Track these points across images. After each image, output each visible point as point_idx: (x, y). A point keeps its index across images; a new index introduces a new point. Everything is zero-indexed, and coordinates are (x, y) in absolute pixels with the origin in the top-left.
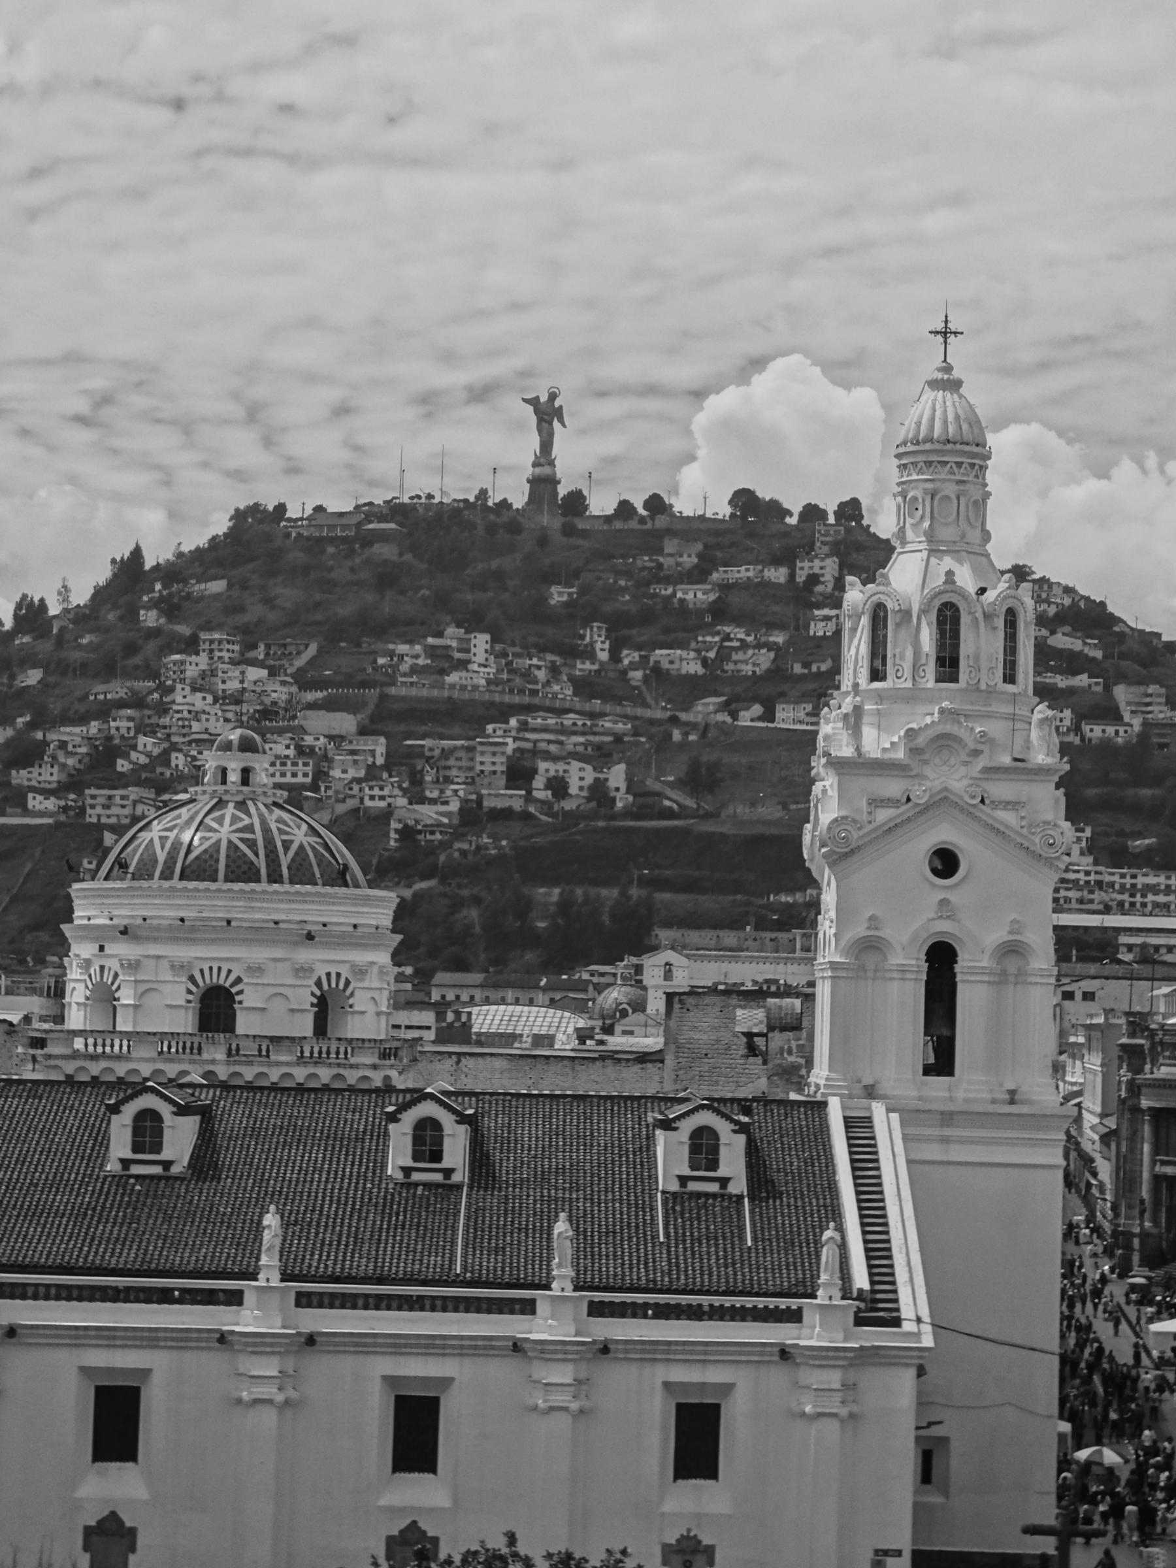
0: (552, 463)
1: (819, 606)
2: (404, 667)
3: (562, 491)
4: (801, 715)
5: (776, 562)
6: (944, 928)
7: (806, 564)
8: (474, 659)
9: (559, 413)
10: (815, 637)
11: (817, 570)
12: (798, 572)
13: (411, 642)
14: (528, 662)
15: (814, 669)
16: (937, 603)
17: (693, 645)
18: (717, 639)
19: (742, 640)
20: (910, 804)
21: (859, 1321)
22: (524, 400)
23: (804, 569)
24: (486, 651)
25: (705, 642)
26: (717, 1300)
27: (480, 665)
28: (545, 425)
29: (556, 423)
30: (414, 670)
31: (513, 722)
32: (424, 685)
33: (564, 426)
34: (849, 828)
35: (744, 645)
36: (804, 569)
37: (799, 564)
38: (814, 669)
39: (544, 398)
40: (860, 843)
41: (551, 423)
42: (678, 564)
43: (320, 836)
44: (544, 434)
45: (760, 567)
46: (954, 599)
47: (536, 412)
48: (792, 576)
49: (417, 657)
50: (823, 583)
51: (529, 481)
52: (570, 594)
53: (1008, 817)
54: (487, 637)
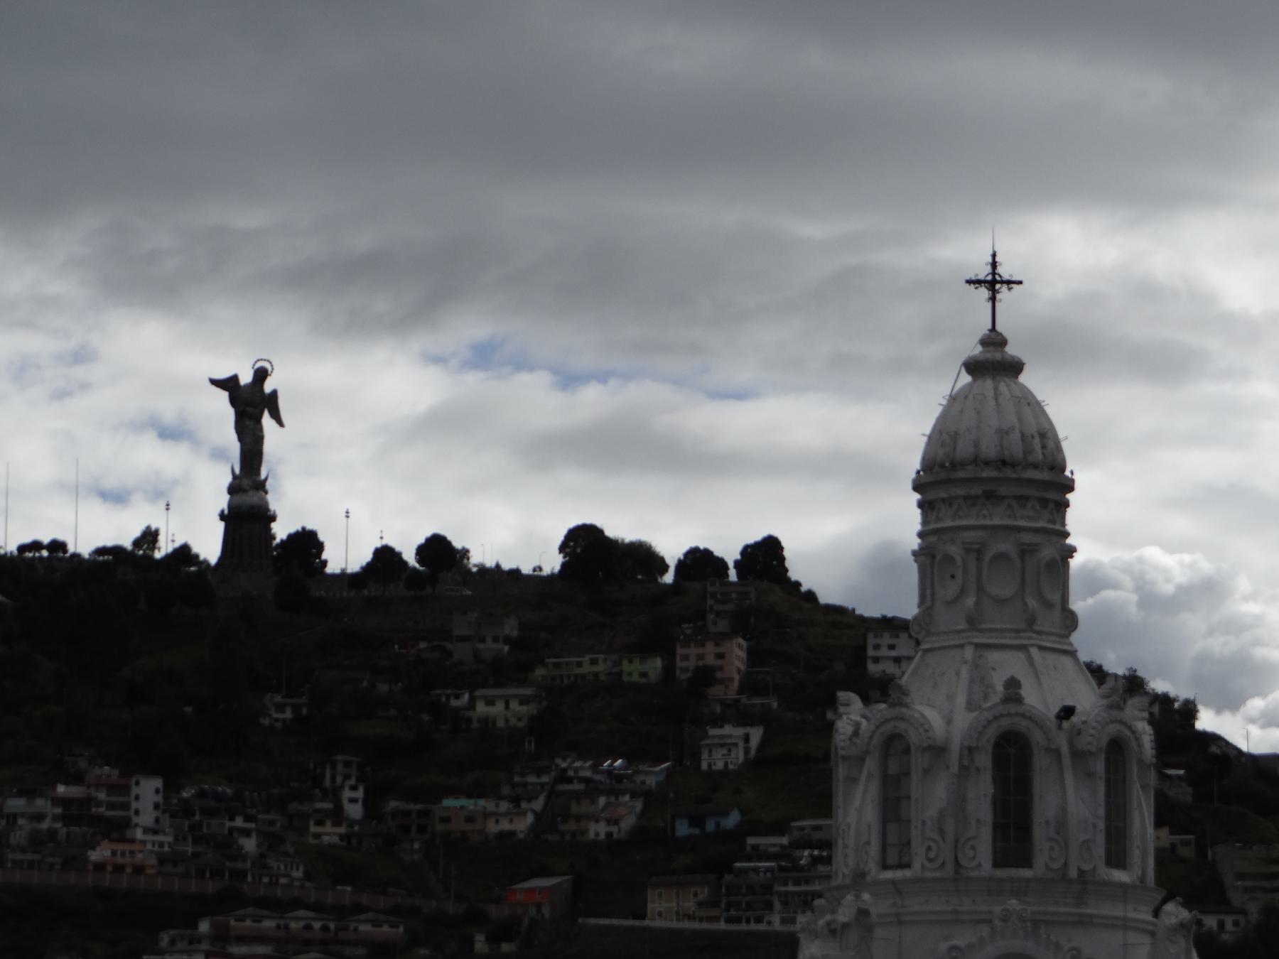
0: (261, 486)
1: (719, 722)
2: (19, 836)
4: (690, 905)
5: (644, 649)
7: (693, 651)
8: (135, 820)
9: (271, 403)
10: (711, 773)
11: (710, 660)
12: (679, 664)
13: (29, 793)
14: (228, 824)
15: (710, 826)
16: (992, 733)
17: (506, 790)
18: (545, 779)
19: (587, 781)
22: (215, 383)
23: (689, 658)
24: (156, 806)
25: (525, 785)
27: (147, 831)
28: (248, 423)
29: (267, 420)
30: (37, 841)
31: (204, 926)
32: (52, 866)
33: (281, 424)
35: (593, 788)
36: (689, 658)
37: (680, 651)
38: (710, 826)
39: (246, 378)
42: (476, 655)
45: (615, 657)
46: (1023, 724)
47: (233, 401)
48: (669, 670)
49: (40, 817)
50: (722, 681)
52: (296, 708)
54: (158, 783)
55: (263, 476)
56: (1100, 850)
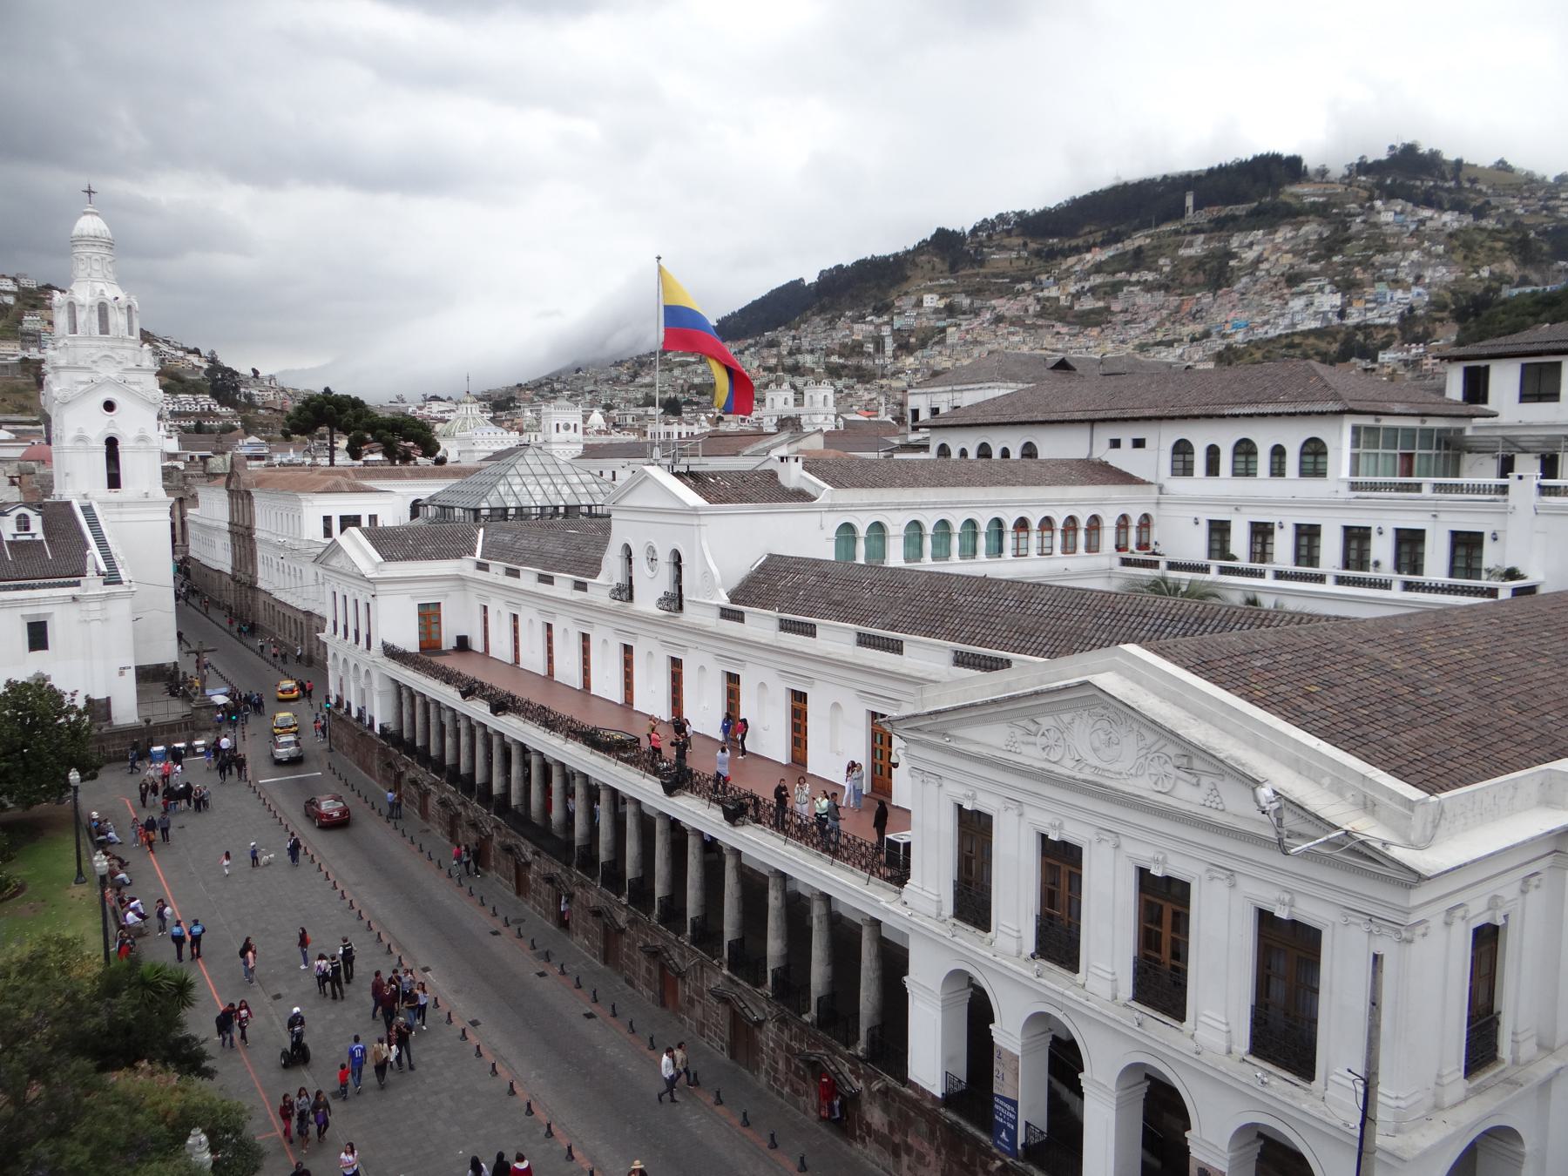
6: (112, 432)
16: (97, 303)
21: (105, 584)
26: (42, 581)
46: (105, 301)
53: (136, 388)
56: (127, 331)
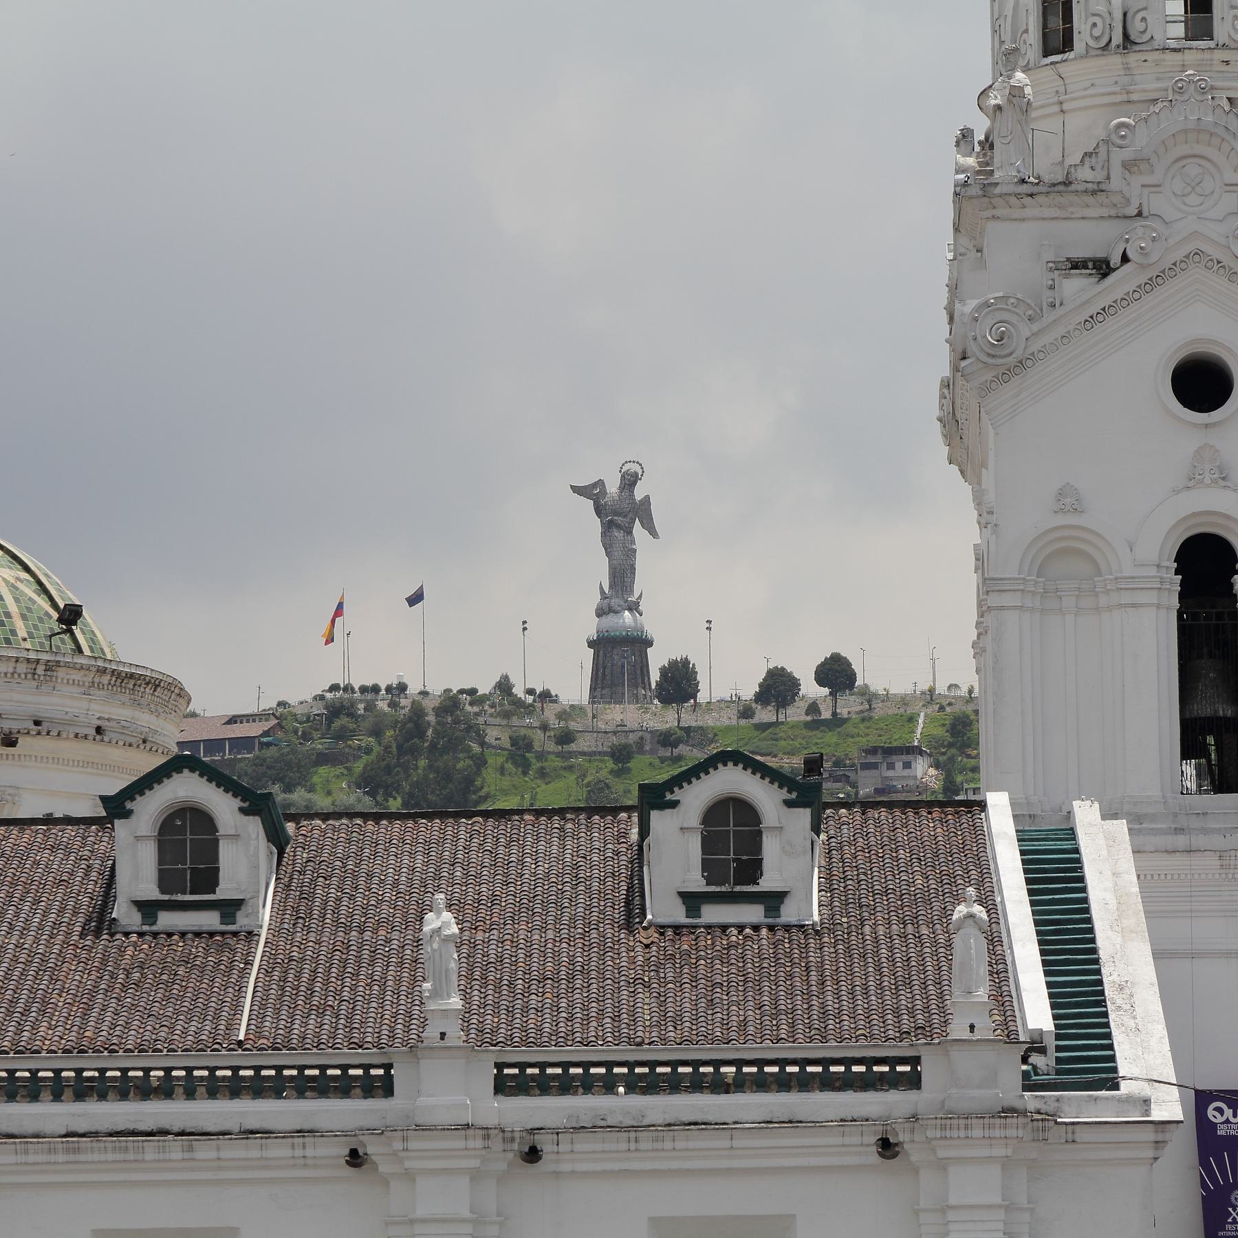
0: (634, 607)
3: (657, 660)
9: (643, 511)
20: (1127, 267)
22: (576, 489)
33: (653, 532)
34: (1013, 318)
40: (1035, 347)
41: (629, 532)
43: (27, 569)
44: (617, 553)
47: (599, 510)
51: (591, 644)
55: (636, 595)
